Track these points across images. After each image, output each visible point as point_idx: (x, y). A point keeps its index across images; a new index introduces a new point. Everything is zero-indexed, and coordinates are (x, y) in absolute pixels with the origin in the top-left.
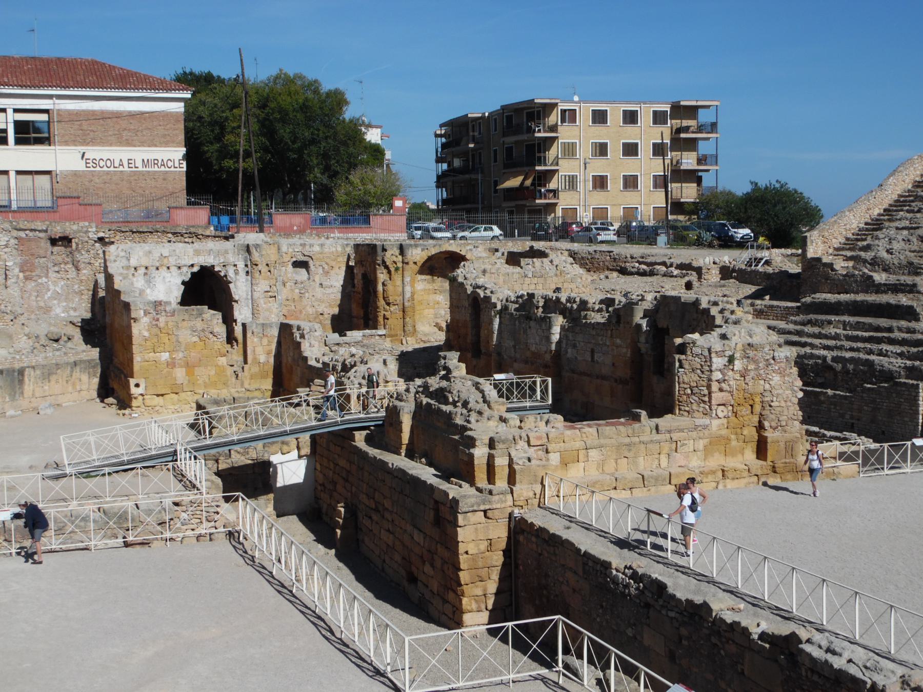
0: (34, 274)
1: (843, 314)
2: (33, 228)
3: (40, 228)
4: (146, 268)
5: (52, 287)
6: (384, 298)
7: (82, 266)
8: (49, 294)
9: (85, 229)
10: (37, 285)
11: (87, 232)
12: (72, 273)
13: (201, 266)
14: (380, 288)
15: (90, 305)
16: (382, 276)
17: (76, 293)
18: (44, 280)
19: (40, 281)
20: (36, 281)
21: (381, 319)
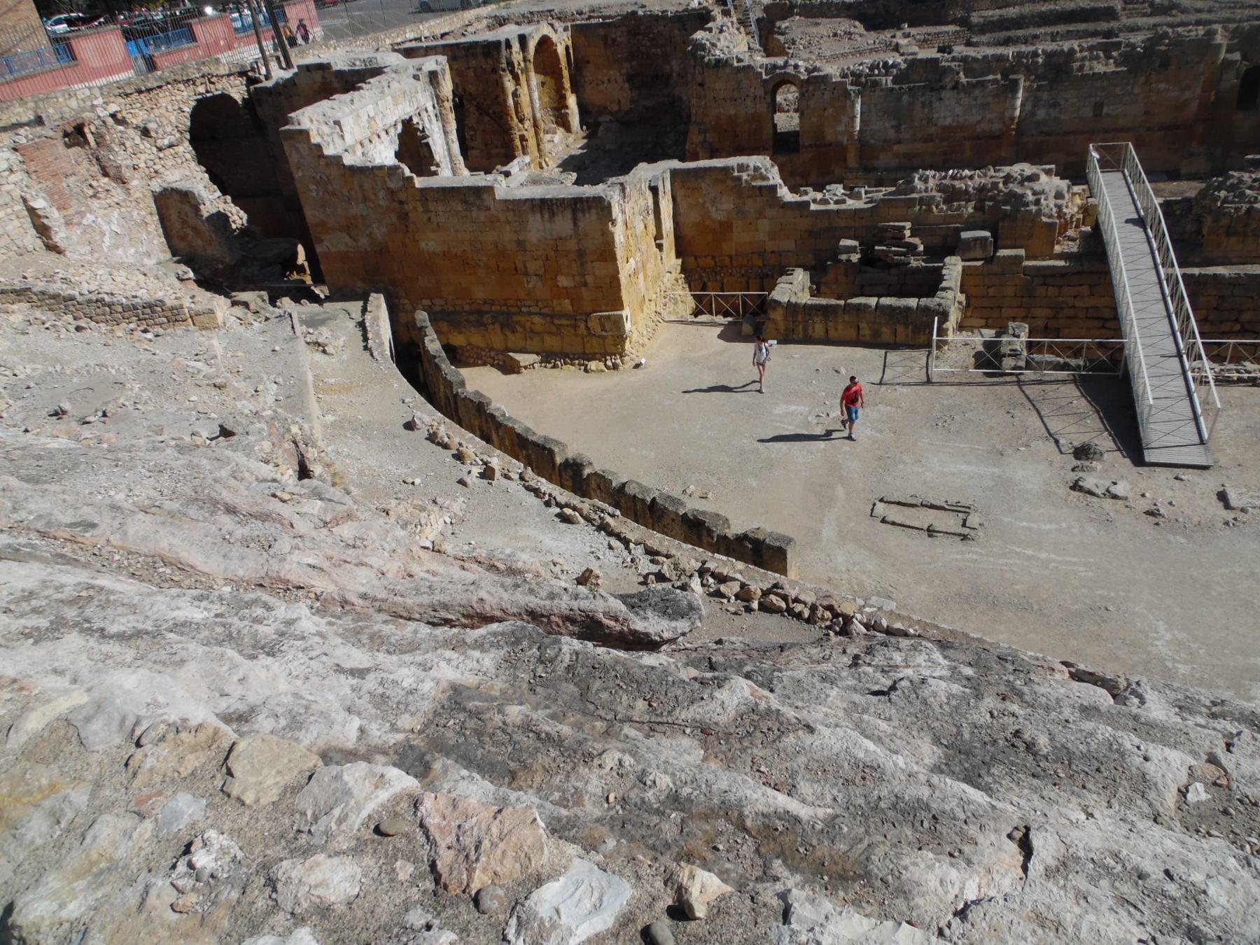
0: (71, 211)
1: (1028, 27)
2: (14, 121)
3: (25, 119)
4: (362, 145)
5: (105, 227)
6: (517, 113)
7: (127, 173)
8: (107, 239)
9: (89, 103)
10: (84, 232)
11: (93, 107)
12: (118, 193)
13: (403, 122)
14: (510, 101)
15: (163, 239)
16: (510, 85)
17: (139, 225)
18: (90, 217)
19: (85, 222)
20: (79, 224)
21: (517, 142)
